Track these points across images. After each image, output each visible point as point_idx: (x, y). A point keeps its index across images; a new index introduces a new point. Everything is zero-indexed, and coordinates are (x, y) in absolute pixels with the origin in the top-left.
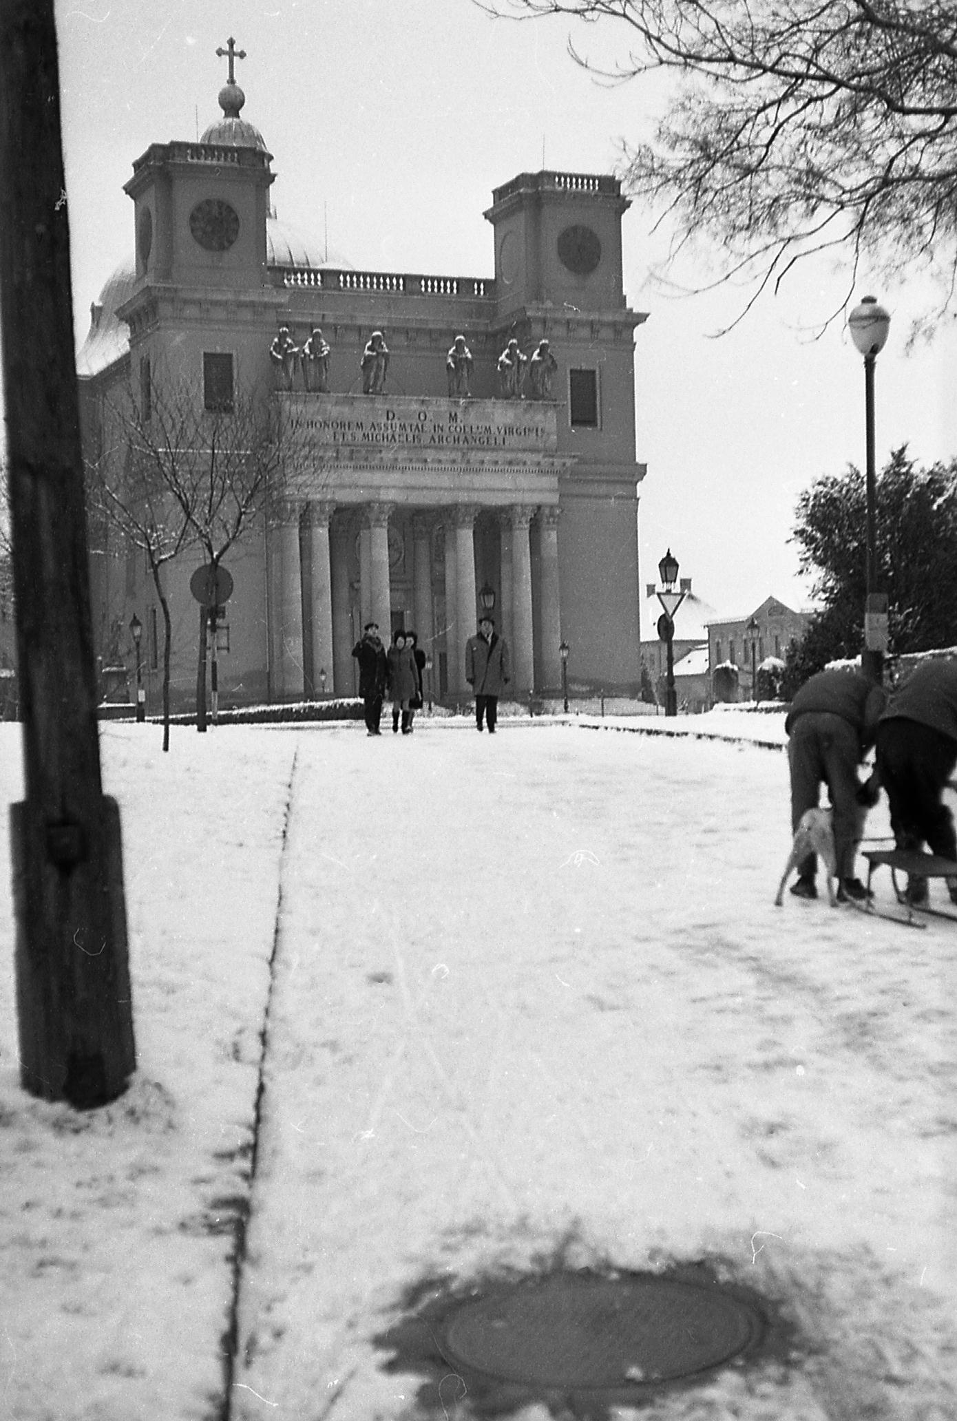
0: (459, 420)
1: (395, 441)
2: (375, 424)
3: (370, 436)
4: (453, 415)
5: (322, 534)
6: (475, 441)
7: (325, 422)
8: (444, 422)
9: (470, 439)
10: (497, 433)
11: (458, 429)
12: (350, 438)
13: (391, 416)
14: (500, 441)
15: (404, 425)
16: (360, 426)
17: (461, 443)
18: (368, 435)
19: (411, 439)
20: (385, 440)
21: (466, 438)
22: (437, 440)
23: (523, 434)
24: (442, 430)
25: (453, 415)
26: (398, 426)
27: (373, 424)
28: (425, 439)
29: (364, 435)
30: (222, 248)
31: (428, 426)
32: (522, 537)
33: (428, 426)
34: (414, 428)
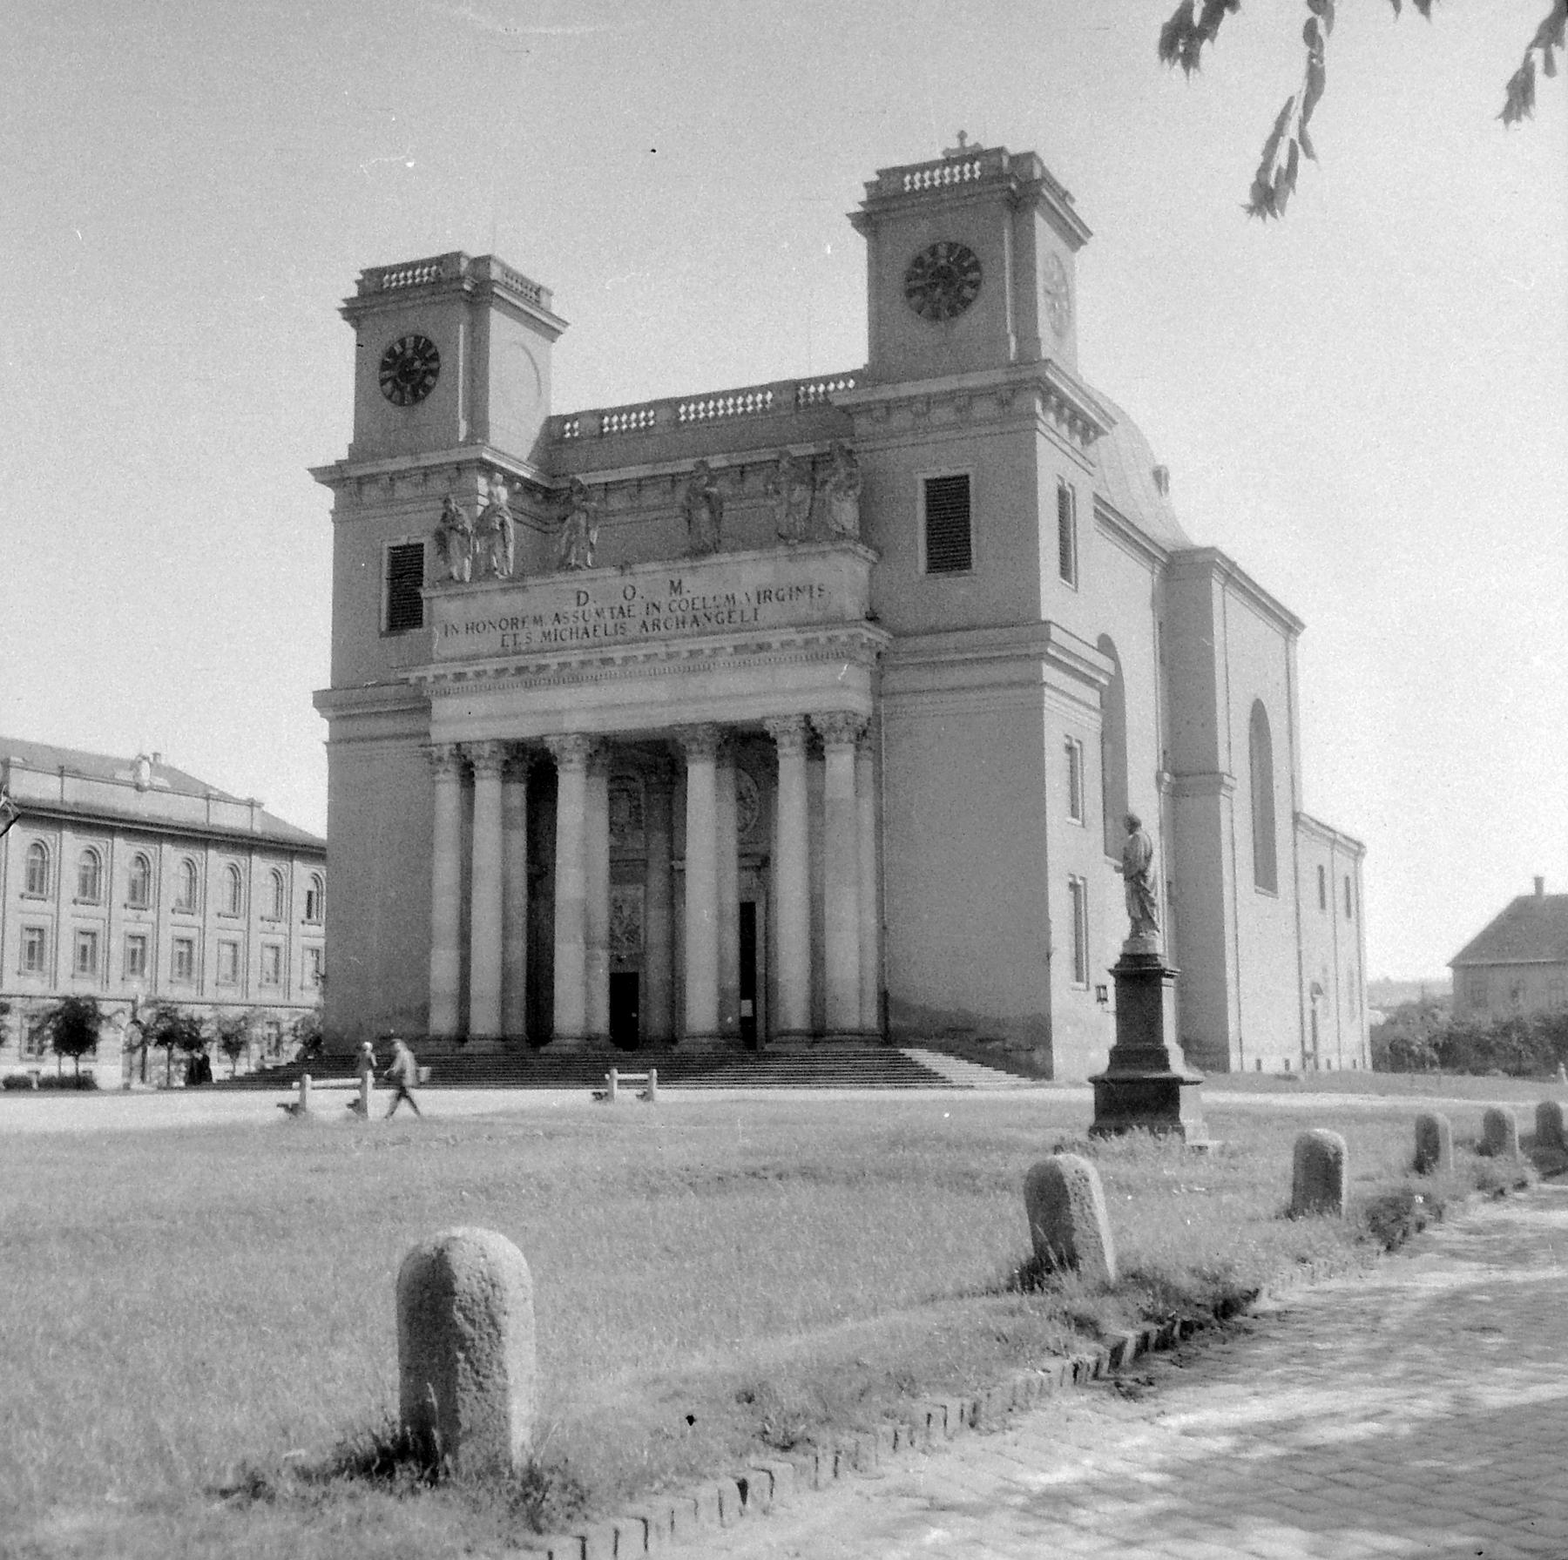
0: (684, 590)
4: (676, 584)
5: (488, 788)
8: (663, 599)
11: (683, 606)
14: (749, 614)
16: (538, 620)
19: (610, 630)
20: (574, 636)
24: (658, 609)
25: (676, 584)
26: (593, 611)
28: (634, 628)
30: (417, 399)
31: (638, 610)
33: (638, 610)
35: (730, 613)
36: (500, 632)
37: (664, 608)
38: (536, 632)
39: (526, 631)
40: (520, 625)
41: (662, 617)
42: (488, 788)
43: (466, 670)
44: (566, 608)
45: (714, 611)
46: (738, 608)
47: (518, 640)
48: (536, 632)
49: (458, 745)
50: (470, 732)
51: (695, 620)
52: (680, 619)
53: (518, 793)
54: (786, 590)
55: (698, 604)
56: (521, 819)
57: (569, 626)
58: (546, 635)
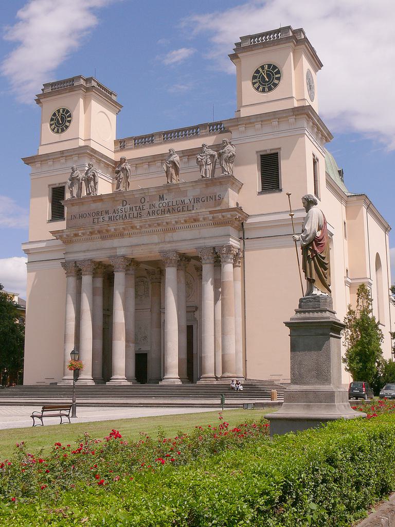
0: (165, 199)
2: (116, 212)
3: (113, 217)
4: (161, 196)
5: (87, 279)
9: (171, 210)
11: (164, 205)
12: (102, 220)
13: (125, 203)
16: (107, 212)
20: (121, 218)
25: (161, 196)
31: (146, 206)
32: (207, 269)
33: (146, 206)
37: (157, 206)
40: (100, 215)
42: (87, 279)
45: (177, 206)
46: (186, 205)
49: (75, 262)
50: (80, 257)
53: (99, 283)
54: (205, 198)
55: (170, 204)
56: (100, 292)
57: (120, 214)
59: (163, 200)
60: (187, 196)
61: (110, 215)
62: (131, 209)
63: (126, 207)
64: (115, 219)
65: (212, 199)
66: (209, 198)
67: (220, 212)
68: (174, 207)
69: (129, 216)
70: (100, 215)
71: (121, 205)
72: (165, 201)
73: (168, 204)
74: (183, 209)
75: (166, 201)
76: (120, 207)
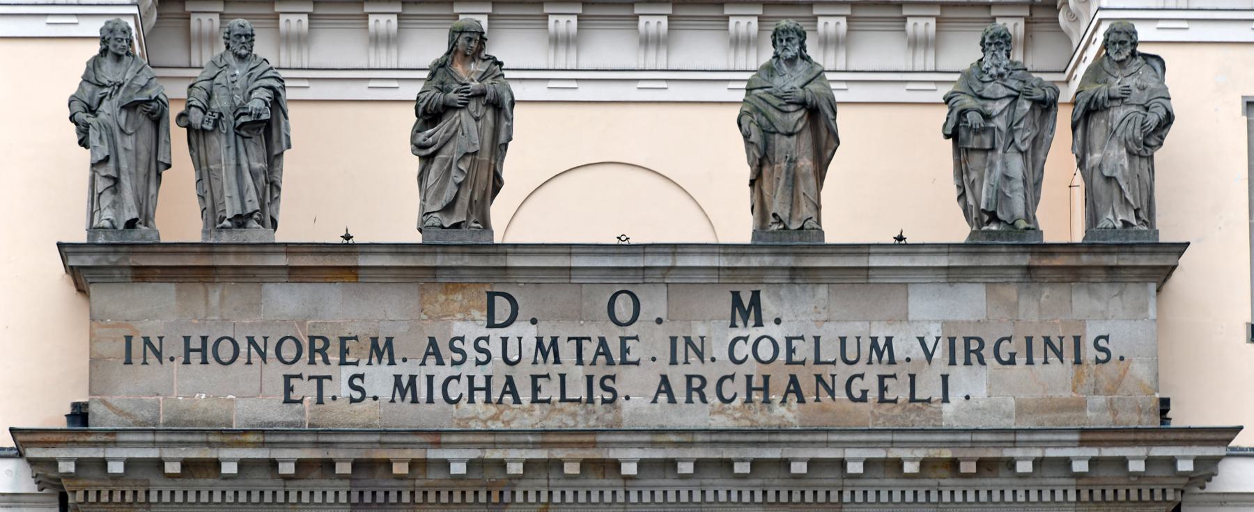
1: (517, 401)
6: (832, 393)
7: (251, 341)
9: (807, 383)
10: (917, 352)
11: (765, 351)
12: (346, 391)
13: (502, 309)
15: (554, 341)
17: (776, 397)
18: (413, 379)
19: (577, 390)
20: (480, 396)
21: (793, 380)
22: (681, 397)
23: (1021, 360)
24: (700, 355)
26: (530, 344)
27: (432, 341)
29: (398, 378)
34: (590, 349)
35: (881, 378)
36: (276, 371)
38: (379, 379)
39: (349, 371)
41: (713, 374)
43: (167, 453)
44: (458, 328)
45: (843, 372)
46: (903, 372)
47: (327, 394)
48: (379, 379)
51: (794, 386)
52: (757, 382)
54: (1018, 345)
55: (804, 351)
57: (467, 369)
58: (404, 388)
59: (759, 323)
60: (904, 318)
61: (404, 370)
62: (547, 349)
63: (511, 332)
64: (438, 394)
65: (1060, 355)
66: (1038, 345)
67: (1135, 443)
68: (826, 371)
69: (536, 389)
70: (334, 358)
71: (482, 316)
72: (769, 329)
73: (791, 351)
74: (883, 389)
75: (779, 333)
76: (470, 328)
